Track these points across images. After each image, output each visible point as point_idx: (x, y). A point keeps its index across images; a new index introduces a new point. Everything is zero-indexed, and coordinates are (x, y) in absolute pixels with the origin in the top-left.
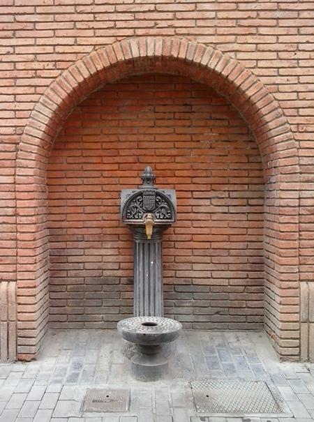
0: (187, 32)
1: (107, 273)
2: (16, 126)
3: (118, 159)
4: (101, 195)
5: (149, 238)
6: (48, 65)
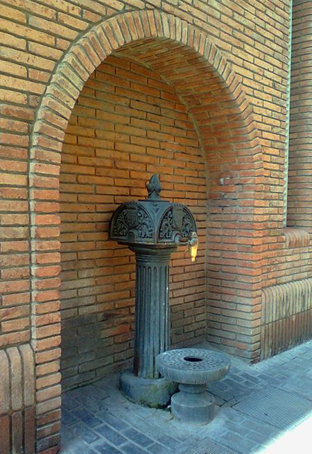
0: (201, 26)
1: (83, 311)
2: (29, 93)
3: (95, 161)
4: (77, 207)
5: (193, 259)
6: (73, 9)
